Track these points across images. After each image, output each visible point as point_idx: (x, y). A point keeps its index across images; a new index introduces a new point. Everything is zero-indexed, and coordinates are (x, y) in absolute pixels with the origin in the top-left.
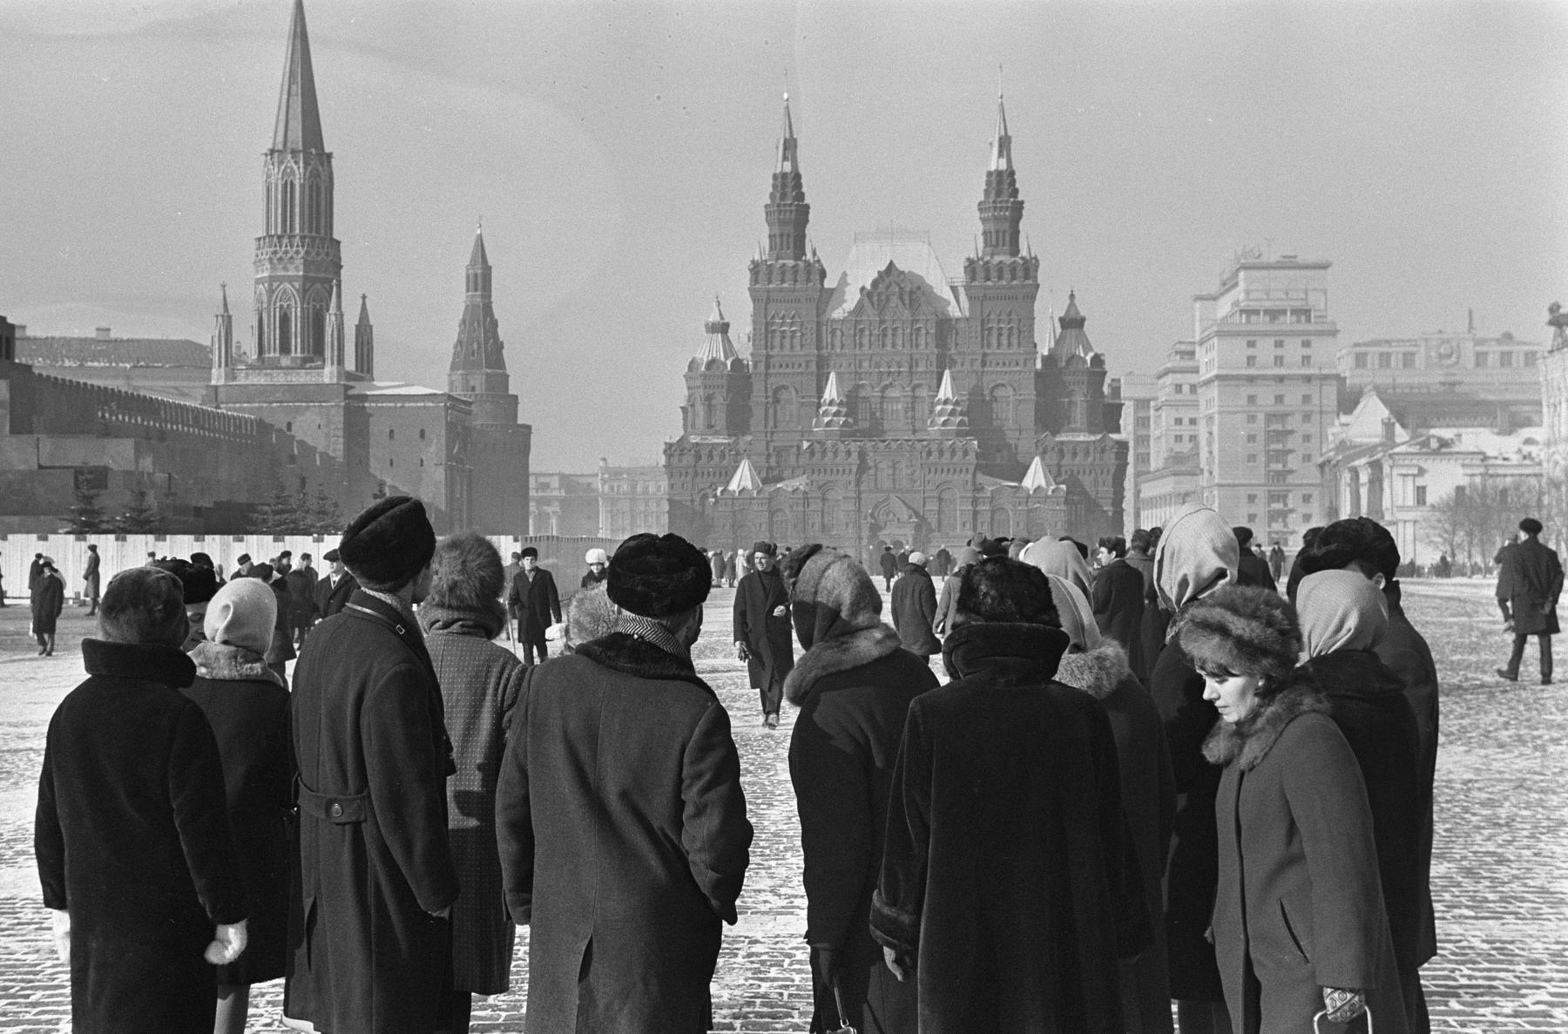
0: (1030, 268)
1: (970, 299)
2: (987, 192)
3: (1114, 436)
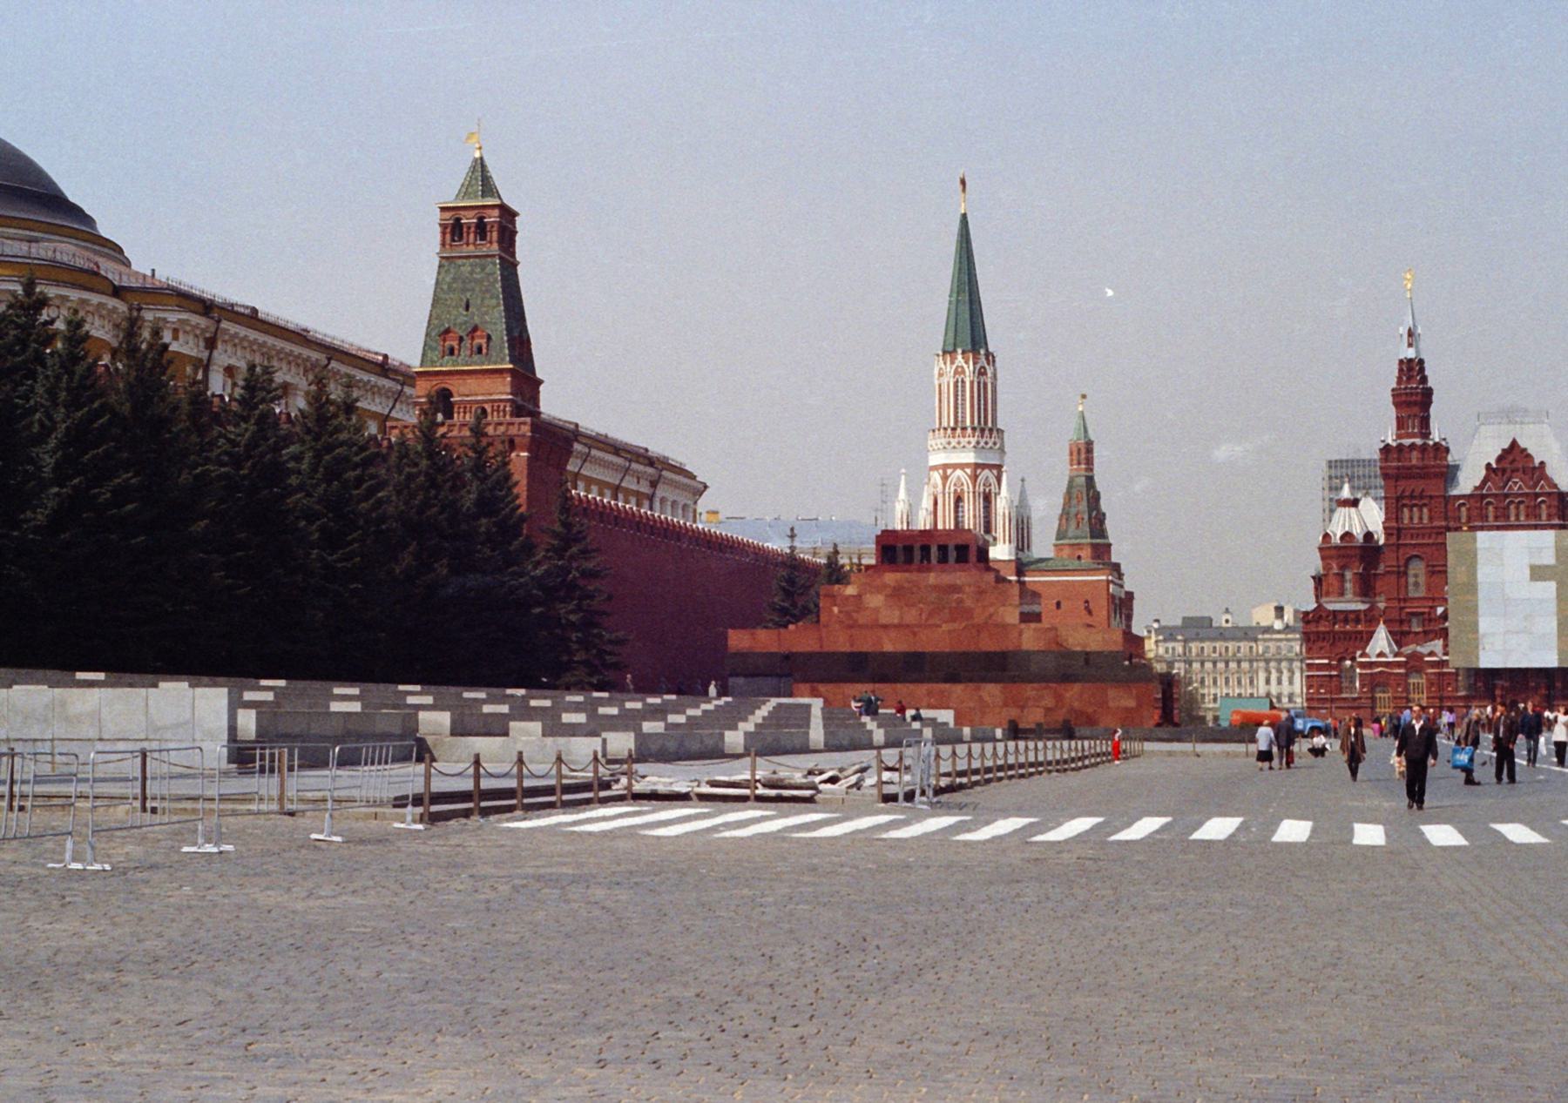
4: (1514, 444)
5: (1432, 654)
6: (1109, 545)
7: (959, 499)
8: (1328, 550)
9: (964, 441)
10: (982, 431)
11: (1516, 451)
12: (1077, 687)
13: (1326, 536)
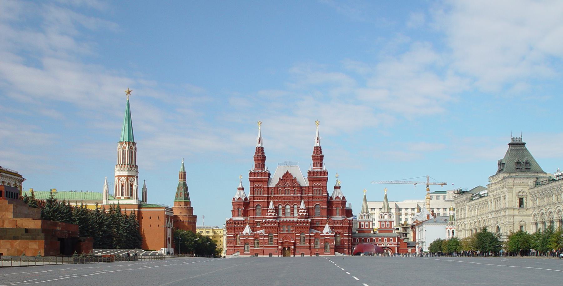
0: (325, 173)
1: (309, 181)
2: (314, 152)
3: (349, 218)
4: (287, 172)
5: (261, 233)
6: (190, 202)
7: (122, 186)
8: (235, 203)
9: (124, 169)
10: (130, 165)
11: (288, 175)
12: (18, 241)
13: (234, 199)
